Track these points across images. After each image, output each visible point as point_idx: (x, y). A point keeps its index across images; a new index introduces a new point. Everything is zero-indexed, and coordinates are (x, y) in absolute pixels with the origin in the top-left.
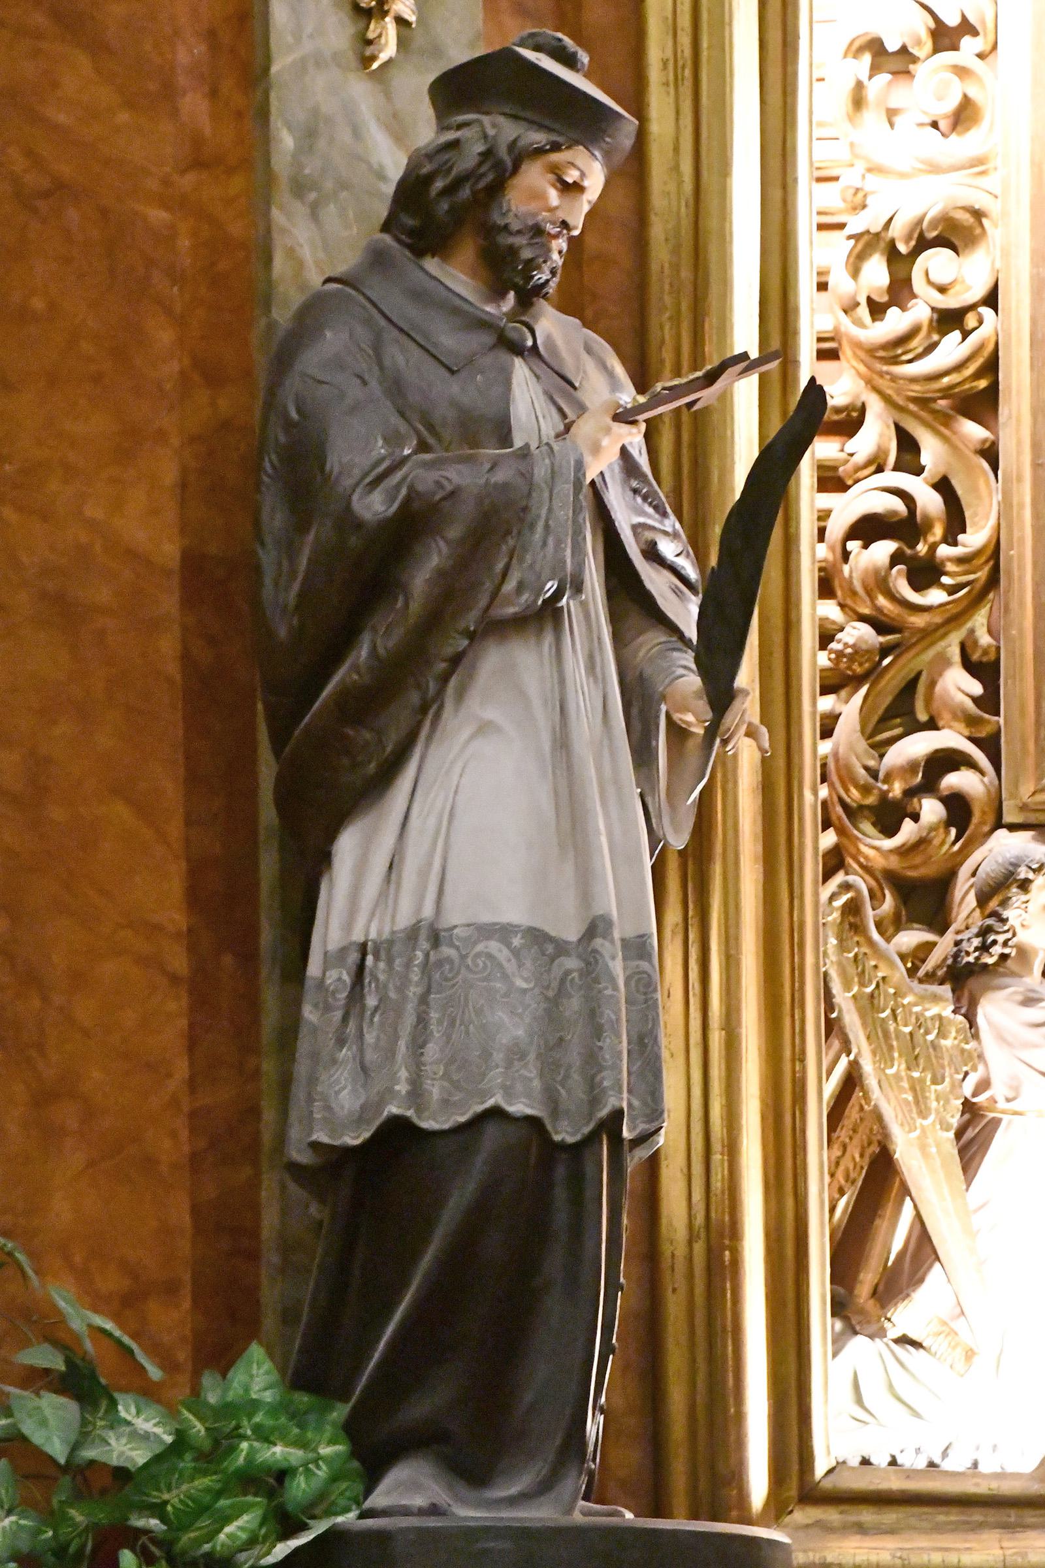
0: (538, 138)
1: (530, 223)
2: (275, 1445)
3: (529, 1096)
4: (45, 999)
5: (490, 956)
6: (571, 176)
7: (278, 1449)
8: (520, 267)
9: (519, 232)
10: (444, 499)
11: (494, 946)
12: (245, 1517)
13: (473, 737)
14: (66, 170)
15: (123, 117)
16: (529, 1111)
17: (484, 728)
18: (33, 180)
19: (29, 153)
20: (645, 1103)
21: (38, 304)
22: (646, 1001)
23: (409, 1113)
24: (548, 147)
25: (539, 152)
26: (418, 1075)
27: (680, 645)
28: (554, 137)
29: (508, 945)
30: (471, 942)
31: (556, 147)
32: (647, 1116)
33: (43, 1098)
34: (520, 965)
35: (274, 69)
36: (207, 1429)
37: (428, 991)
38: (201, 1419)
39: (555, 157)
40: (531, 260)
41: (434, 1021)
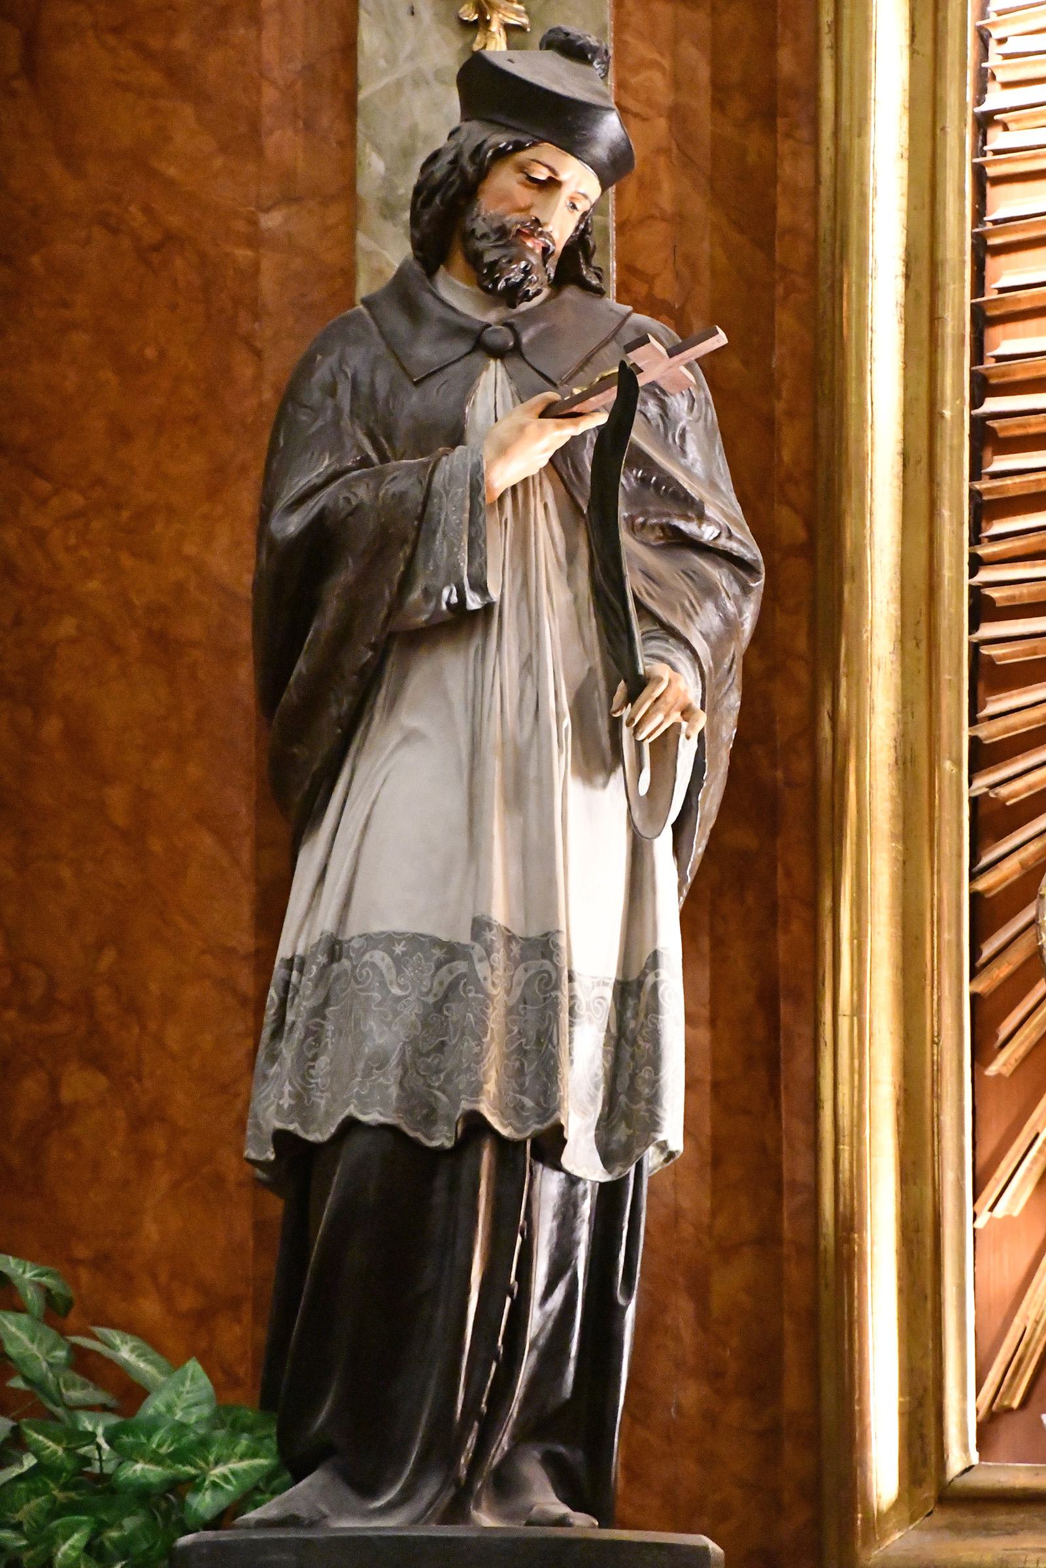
0: (502, 140)
1: (496, 225)
2: (137, 1462)
3: (384, 1103)
4: (143, 1027)
5: (374, 966)
6: (542, 174)
7: (139, 1467)
8: (485, 271)
10: (351, 514)
11: (379, 957)
12: (76, 1536)
13: (398, 746)
14: (175, 221)
15: (218, 162)
16: (382, 1119)
17: (410, 737)
18: (151, 235)
19: (147, 210)
20: (538, 1104)
21: (150, 353)
22: (545, 999)
23: (291, 1127)
24: (510, 147)
25: (501, 155)
26: (304, 1089)
27: (661, 633)
28: (513, 137)
29: (391, 953)
30: (361, 952)
31: (519, 147)
32: (538, 1116)
33: (139, 1123)
34: (399, 972)
35: (362, 96)
36: (65, 1449)
37: (326, 1003)
38: (57, 1441)
39: (523, 156)
40: (495, 263)
41: (330, 1034)
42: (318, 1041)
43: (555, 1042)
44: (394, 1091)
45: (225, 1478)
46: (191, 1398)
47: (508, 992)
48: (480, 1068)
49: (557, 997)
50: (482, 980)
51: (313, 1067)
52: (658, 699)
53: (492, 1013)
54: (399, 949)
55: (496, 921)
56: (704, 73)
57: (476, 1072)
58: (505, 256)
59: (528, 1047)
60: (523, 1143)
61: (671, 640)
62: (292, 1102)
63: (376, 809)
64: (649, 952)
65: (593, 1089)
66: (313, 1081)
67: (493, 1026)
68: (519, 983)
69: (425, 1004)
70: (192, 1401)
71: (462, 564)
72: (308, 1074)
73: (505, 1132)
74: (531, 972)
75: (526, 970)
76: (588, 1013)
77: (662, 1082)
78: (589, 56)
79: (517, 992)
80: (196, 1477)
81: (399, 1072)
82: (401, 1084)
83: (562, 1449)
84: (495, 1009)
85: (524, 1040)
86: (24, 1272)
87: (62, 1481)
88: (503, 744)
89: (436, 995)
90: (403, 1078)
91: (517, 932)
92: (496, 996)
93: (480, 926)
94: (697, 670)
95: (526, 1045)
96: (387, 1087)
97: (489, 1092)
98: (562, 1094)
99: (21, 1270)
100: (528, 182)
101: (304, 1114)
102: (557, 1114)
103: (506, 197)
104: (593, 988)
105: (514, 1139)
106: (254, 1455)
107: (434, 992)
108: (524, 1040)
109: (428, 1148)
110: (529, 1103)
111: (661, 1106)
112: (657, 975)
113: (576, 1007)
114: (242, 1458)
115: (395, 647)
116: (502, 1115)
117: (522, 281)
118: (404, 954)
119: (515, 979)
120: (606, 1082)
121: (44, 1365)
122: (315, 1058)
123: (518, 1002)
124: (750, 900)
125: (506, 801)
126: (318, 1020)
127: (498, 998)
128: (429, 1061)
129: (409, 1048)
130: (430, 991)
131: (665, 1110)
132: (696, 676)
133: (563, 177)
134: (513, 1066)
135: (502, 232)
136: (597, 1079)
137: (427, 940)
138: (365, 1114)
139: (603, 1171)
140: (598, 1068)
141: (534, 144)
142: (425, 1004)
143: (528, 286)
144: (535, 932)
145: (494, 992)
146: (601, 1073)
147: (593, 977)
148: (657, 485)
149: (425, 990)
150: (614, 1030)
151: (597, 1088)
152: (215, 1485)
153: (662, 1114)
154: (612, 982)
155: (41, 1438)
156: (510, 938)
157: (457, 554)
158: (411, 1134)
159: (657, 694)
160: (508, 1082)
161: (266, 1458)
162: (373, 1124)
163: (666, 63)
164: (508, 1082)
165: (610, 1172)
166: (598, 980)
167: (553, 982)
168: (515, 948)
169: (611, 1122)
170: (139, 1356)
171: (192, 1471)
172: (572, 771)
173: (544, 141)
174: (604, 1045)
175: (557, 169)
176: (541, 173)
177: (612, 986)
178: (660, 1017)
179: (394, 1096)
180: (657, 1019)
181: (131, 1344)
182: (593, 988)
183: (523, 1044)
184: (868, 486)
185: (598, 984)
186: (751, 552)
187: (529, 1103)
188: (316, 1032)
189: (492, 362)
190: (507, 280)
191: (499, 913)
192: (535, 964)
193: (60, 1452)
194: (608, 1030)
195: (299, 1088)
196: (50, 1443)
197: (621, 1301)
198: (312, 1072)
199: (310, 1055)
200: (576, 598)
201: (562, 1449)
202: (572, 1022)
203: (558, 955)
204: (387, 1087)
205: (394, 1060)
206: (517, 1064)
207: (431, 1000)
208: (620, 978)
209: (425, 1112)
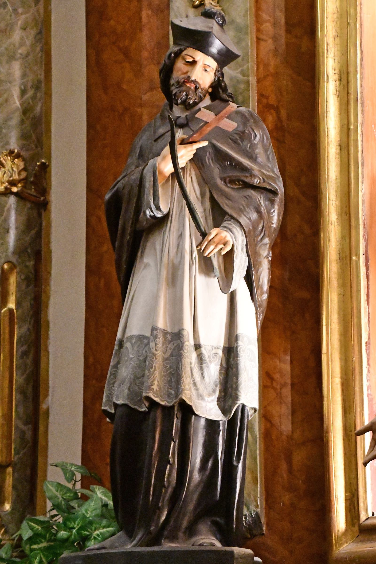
6: (190, 60)
9: (173, 85)
13: (143, 269)
20: (175, 392)
24: (178, 52)
26: (110, 394)
29: (131, 342)
40: (176, 93)
42: (115, 377)
43: (180, 369)
44: (126, 392)
45: (98, 535)
46: (94, 507)
47: (164, 353)
48: (149, 381)
49: (181, 353)
50: (151, 349)
51: (113, 386)
52: (211, 240)
53: (155, 361)
54: (133, 341)
55: (159, 327)
56: (283, 20)
57: (148, 382)
58: (178, 91)
59: (173, 372)
60: (173, 407)
61: (232, 220)
62: (106, 399)
63: (136, 293)
64: (235, 335)
65: (214, 387)
66: (113, 391)
67: (155, 365)
68: (170, 349)
69: (139, 360)
70: (93, 509)
71: (150, 200)
72: (111, 388)
73: (163, 403)
74: (175, 345)
75: (173, 344)
76: (208, 359)
77: (239, 382)
78: (212, 16)
79: (169, 352)
80: (88, 535)
81: (128, 385)
82: (129, 389)
83: (218, 519)
84: (156, 359)
85: (172, 370)
86: (72, 468)
87: (47, 539)
88: (168, 264)
89: (143, 356)
90: (129, 387)
91: (169, 330)
92: (157, 354)
93: (154, 329)
94: (242, 230)
95: (173, 371)
96: (124, 391)
97: (154, 389)
98: (183, 388)
99: (70, 467)
100: (186, 63)
101: (110, 403)
102: (180, 396)
103: (180, 70)
104: (212, 350)
105: (168, 406)
106: (108, 527)
107: (143, 355)
108: (172, 370)
109: (141, 411)
110: (173, 392)
111: (239, 391)
112: (237, 343)
113: (203, 357)
114: (104, 527)
115: (145, 234)
116: (161, 397)
117: (187, 98)
118: (135, 342)
119: (168, 348)
120: (221, 384)
121: (61, 499)
122: (114, 383)
123: (170, 356)
124: (307, 316)
125: (168, 284)
126: (115, 369)
127: (158, 355)
128: (140, 380)
129: (132, 376)
130: (142, 355)
131: (240, 392)
132: (242, 232)
133: (196, 59)
134: (168, 379)
135: (178, 82)
136: (216, 383)
137: (142, 337)
138: (118, 401)
139: (223, 417)
140: (217, 379)
141: (185, 49)
142: (139, 360)
143: (189, 100)
144: (176, 330)
145: (157, 353)
146: (218, 381)
147: (212, 346)
148: (235, 166)
149: (140, 355)
150: (224, 365)
151: (216, 386)
152: (95, 538)
153: (239, 394)
154: (222, 347)
155: (33, 524)
156: (165, 333)
157: (149, 197)
158: (132, 406)
159: (210, 238)
160: (165, 385)
161: (112, 527)
162: (120, 404)
163: (272, 20)
164: (165, 385)
165: (226, 417)
166: (215, 347)
167: (180, 348)
168: (169, 337)
169: (226, 399)
170: (103, 494)
171: (87, 533)
172: (199, 272)
173: (189, 47)
174: (220, 370)
175: (194, 56)
176: (189, 59)
177: (222, 349)
178: (238, 359)
179: (126, 393)
180: (237, 359)
181: (101, 491)
182: (212, 350)
183: (172, 371)
184: (326, 158)
185: (215, 349)
186: (279, 186)
187: (173, 392)
188: (115, 374)
189: (179, 130)
190: (181, 99)
191: (161, 324)
192: (176, 343)
193: (40, 528)
194: (221, 364)
195: (108, 394)
196: (36, 526)
197: (235, 463)
198: (113, 388)
199: (112, 382)
200: (205, 210)
201: (218, 519)
202: (202, 363)
203: (182, 338)
204: (124, 391)
205: (127, 380)
206: (169, 378)
207: (142, 358)
208: (227, 346)
209: (139, 398)
